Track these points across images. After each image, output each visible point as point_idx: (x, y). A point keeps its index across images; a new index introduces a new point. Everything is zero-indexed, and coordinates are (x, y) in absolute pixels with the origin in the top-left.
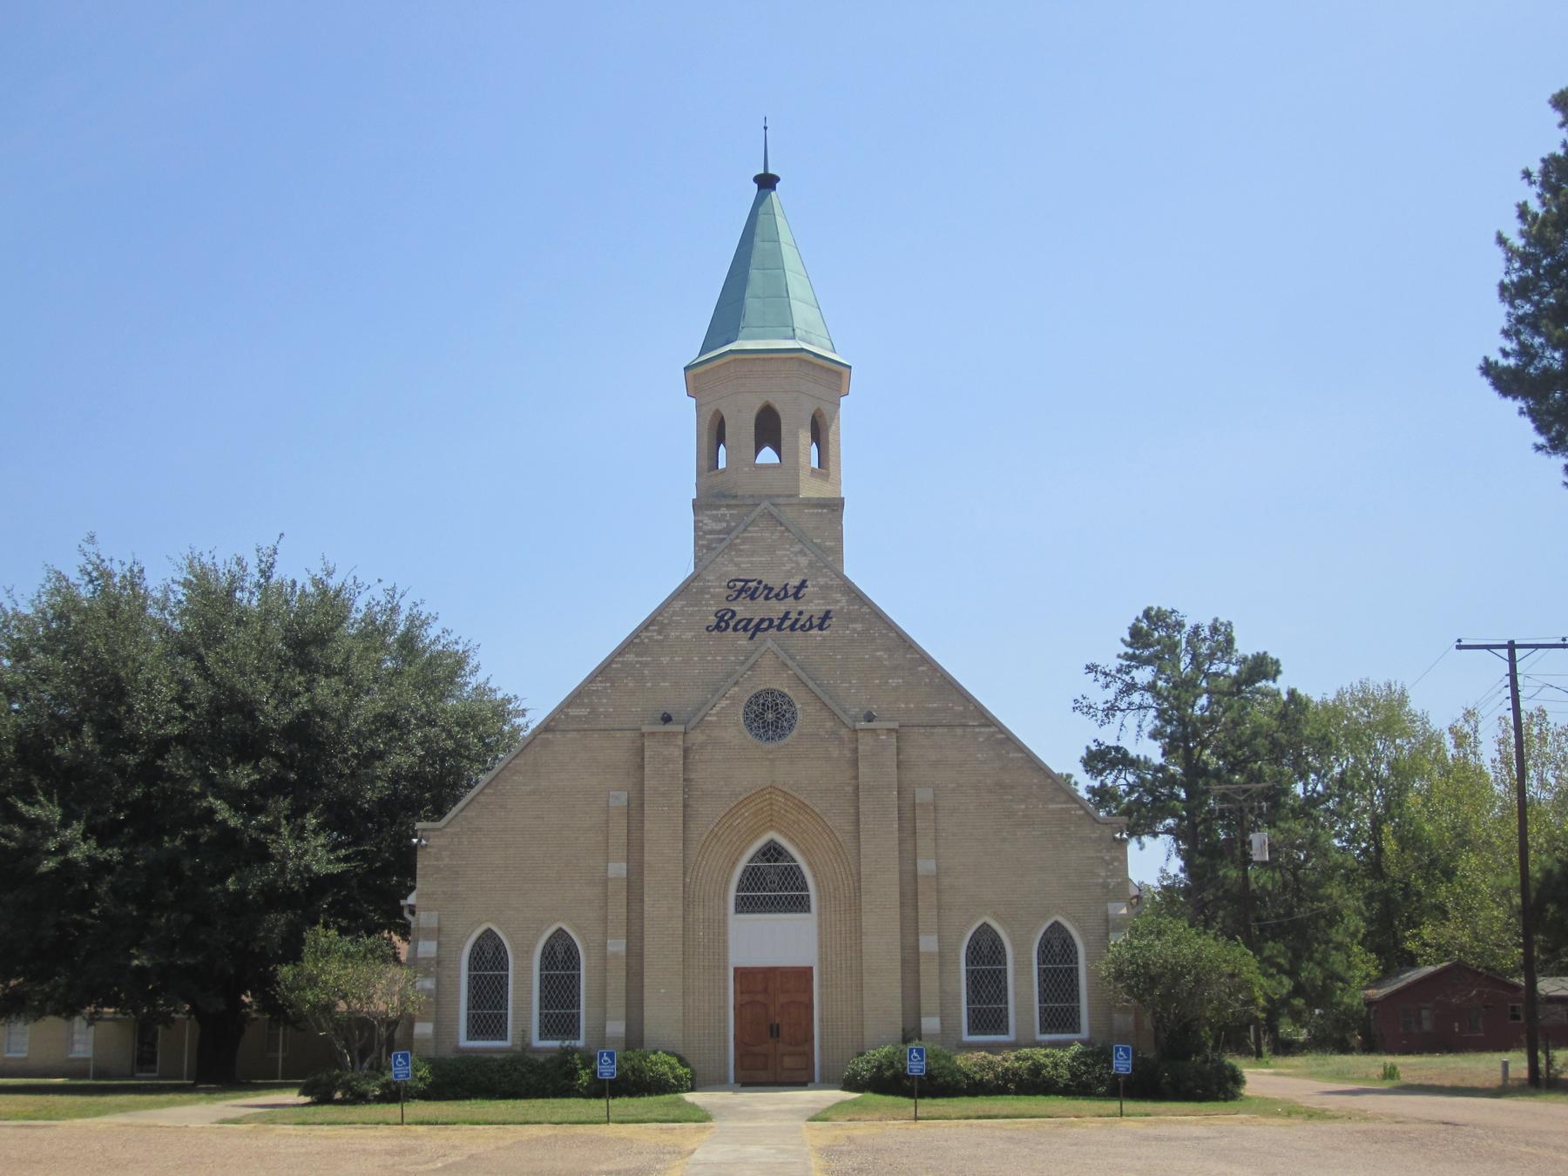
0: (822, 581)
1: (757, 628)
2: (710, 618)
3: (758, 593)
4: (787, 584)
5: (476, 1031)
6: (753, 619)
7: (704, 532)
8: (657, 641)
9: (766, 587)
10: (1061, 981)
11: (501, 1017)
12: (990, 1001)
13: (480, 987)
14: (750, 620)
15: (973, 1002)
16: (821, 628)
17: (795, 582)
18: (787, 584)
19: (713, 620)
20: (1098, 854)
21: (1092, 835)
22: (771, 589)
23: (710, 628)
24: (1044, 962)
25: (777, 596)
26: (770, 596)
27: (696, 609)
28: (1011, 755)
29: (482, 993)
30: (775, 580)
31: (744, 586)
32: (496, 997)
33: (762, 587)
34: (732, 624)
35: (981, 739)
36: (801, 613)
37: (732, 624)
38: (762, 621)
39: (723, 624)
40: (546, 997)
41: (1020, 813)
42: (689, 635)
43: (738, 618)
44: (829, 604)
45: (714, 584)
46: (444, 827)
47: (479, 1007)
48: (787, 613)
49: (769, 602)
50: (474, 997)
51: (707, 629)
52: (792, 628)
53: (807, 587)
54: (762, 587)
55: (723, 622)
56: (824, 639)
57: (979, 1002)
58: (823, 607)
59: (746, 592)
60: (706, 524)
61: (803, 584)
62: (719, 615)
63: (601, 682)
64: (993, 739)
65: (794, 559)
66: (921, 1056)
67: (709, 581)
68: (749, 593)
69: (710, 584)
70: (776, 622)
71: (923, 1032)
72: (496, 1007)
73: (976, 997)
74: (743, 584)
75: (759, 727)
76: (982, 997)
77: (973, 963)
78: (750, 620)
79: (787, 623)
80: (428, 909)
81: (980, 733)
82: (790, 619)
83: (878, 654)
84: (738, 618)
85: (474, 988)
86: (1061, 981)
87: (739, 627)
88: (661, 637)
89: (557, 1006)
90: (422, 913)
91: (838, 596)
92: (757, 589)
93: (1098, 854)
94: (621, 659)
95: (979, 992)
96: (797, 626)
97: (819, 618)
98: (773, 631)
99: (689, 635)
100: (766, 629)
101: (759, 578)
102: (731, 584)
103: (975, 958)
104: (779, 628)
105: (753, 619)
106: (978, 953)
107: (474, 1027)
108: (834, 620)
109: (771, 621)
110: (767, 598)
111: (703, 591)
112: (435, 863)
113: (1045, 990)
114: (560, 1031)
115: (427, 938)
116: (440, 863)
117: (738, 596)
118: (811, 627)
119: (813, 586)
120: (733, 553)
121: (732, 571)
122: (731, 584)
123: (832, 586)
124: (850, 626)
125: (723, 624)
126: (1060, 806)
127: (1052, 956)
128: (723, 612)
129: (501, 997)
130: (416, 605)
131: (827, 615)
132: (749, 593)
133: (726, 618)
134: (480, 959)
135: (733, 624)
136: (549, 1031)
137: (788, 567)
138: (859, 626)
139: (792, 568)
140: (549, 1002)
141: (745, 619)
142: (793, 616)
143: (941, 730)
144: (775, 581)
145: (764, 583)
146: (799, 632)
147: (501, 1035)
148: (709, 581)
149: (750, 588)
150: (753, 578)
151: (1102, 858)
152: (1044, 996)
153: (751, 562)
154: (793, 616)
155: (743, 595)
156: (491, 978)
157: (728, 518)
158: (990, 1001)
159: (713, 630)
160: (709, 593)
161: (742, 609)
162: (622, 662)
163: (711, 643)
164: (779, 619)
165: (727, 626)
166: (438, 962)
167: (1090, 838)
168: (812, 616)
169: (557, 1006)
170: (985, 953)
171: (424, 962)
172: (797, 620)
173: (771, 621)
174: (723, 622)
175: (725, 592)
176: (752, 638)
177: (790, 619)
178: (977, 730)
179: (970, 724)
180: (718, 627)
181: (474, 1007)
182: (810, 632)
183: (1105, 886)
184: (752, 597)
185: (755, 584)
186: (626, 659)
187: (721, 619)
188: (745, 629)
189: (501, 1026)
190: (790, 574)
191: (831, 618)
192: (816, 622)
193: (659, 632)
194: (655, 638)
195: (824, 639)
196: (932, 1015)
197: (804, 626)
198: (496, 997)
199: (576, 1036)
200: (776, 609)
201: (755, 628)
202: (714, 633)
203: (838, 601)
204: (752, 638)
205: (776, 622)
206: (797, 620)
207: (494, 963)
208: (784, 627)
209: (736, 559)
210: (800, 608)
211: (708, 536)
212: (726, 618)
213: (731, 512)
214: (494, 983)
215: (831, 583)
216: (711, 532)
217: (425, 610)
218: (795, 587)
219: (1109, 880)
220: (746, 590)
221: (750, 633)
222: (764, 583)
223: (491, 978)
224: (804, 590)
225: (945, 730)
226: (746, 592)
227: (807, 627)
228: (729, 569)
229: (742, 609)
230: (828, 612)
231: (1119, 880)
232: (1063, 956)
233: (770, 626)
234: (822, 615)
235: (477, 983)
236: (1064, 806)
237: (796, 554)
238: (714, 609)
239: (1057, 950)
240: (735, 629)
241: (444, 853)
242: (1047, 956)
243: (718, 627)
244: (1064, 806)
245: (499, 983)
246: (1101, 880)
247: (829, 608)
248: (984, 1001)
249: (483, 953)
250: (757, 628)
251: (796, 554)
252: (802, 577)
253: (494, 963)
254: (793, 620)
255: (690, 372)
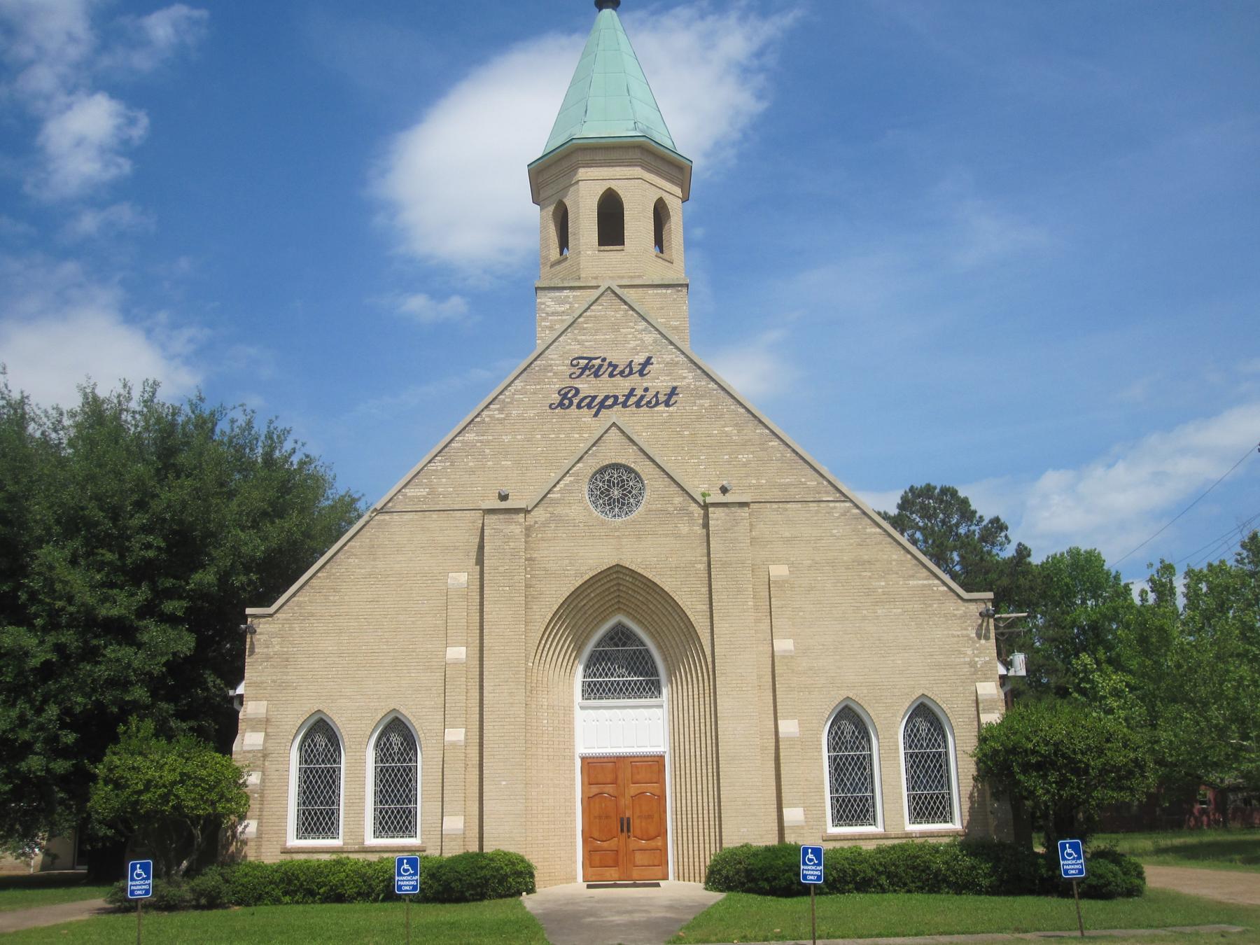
0: (667, 358)
1: (602, 405)
2: (553, 396)
3: (602, 370)
4: (632, 361)
5: (306, 829)
6: (597, 396)
7: (547, 313)
8: (498, 419)
9: (610, 364)
10: (929, 766)
11: (333, 813)
12: (854, 790)
13: (311, 782)
14: (594, 398)
15: (837, 791)
16: (667, 404)
17: (641, 359)
18: (632, 361)
19: (556, 398)
20: (965, 632)
21: (956, 612)
22: (615, 367)
23: (553, 406)
24: (910, 747)
25: (622, 373)
26: (615, 373)
27: (538, 387)
28: (868, 530)
29: (313, 787)
30: (619, 357)
31: (588, 364)
32: (328, 792)
33: (606, 364)
34: (576, 401)
35: (836, 515)
36: (646, 390)
37: (576, 401)
38: (607, 398)
39: (566, 402)
40: (381, 791)
41: (880, 590)
42: (531, 413)
43: (581, 395)
44: (675, 380)
45: (557, 362)
46: (275, 613)
47: (310, 803)
48: (633, 390)
49: (613, 379)
50: (305, 793)
51: (550, 406)
52: (638, 404)
53: (652, 364)
54: (606, 364)
55: (566, 399)
56: (671, 415)
57: (843, 790)
58: (670, 384)
59: (590, 369)
60: (548, 306)
61: (648, 361)
62: (563, 392)
63: (440, 461)
64: (848, 514)
65: (640, 336)
66: (819, 858)
67: (552, 359)
68: (593, 370)
69: (552, 362)
70: (621, 399)
71: (785, 825)
72: (327, 803)
73: (840, 785)
74: (587, 361)
75: (627, 481)
76: (845, 785)
77: (834, 749)
78: (594, 398)
79: (633, 400)
80: (257, 699)
81: (835, 508)
82: (636, 395)
83: (726, 429)
84: (581, 395)
85: (305, 782)
86: (929, 766)
87: (583, 404)
88: (503, 416)
89: (392, 801)
90: (249, 703)
91: (685, 373)
92: (601, 366)
93: (965, 632)
94: (461, 438)
95: (842, 780)
96: (643, 403)
97: (665, 395)
98: (618, 408)
99: (531, 413)
100: (610, 407)
101: (603, 355)
102: (575, 362)
103: (837, 743)
104: (625, 405)
105: (597, 396)
106: (840, 738)
107: (304, 824)
108: (681, 396)
109: (616, 398)
110: (611, 375)
111: (546, 369)
112: (266, 650)
113: (913, 777)
114: (395, 828)
115: (254, 729)
116: (270, 650)
117: (581, 374)
118: (657, 404)
119: (658, 363)
120: (576, 332)
121: (577, 350)
122: (575, 362)
123: (677, 363)
124: (697, 401)
125: (566, 402)
126: (921, 582)
127: (918, 741)
128: (567, 390)
129: (334, 792)
130: (271, 422)
131: (674, 392)
132: (593, 370)
133: (569, 395)
134: (312, 751)
135: (577, 401)
136: (383, 828)
137: (633, 344)
138: (707, 403)
139: (637, 346)
140: (384, 796)
141: (590, 396)
142: (639, 392)
143: (794, 506)
144: (620, 358)
145: (608, 361)
146: (645, 408)
147: (332, 833)
148: (552, 359)
149: (594, 366)
150: (597, 355)
151: (968, 636)
152: (913, 783)
153: (595, 341)
154: (639, 392)
155: (587, 372)
156: (323, 772)
157: (571, 300)
158: (854, 790)
159: (556, 408)
160: (550, 371)
161: (586, 386)
162: (462, 442)
163: (554, 420)
164: (623, 396)
165: (571, 403)
166: (265, 755)
167: (955, 615)
168: (658, 393)
169: (392, 801)
170: (848, 738)
171: (251, 755)
172: (642, 397)
173: (616, 398)
174: (566, 399)
175: (567, 370)
176: (596, 415)
177: (636, 395)
178: (832, 505)
179: (824, 499)
180: (561, 405)
181: (304, 803)
182: (656, 409)
183: (972, 664)
184: (596, 375)
185: (599, 361)
186: (466, 439)
187: (565, 396)
188: (589, 406)
189: (333, 824)
190: (635, 351)
191: (677, 394)
192: (662, 398)
193: (501, 410)
194: (497, 416)
195: (671, 415)
196: (795, 806)
197: (650, 402)
198: (328, 792)
199: (413, 833)
200: (621, 386)
201: (600, 405)
202: (557, 411)
203: (685, 378)
204: (596, 415)
205: (621, 399)
206: (642, 397)
207: (326, 756)
208: (629, 403)
209: (579, 338)
210: (645, 385)
211: (550, 318)
212: (569, 395)
213: (574, 293)
214: (325, 777)
215: (676, 359)
216: (553, 314)
217: (280, 425)
218: (639, 364)
219: (977, 659)
220: (589, 367)
221: (595, 410)
222: (608, 361)
223: (323, 772)
224: (649, 368)
225: (799, 505)
226: (590, 369)
227: (653, 403)
228: (573, 347)
229: (586, 386)
230: (675, 388)
231: (987, 659)
232: (930, 740)
233: (615, 403)
234: (669, 391)
235: (308, 777)
236: (925, 582)
237: (640, 332)
238: (557, 386)
239: (924, 735)
240: (579, 407)
241: (275, 641)
242: (913, 741)
243: (561, 405)
244: (925, 582)
245: (331, 777)
246: (967, 659)
247: (675, 384)
248: (849, 789)
249: (315, 746)
250: (602, 405)
251: (640, 332)
252: (647, 355)
253: (326, 756)
254: (638, 396)
255: (530, 167)
